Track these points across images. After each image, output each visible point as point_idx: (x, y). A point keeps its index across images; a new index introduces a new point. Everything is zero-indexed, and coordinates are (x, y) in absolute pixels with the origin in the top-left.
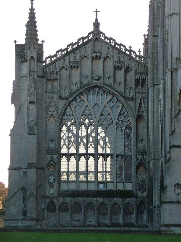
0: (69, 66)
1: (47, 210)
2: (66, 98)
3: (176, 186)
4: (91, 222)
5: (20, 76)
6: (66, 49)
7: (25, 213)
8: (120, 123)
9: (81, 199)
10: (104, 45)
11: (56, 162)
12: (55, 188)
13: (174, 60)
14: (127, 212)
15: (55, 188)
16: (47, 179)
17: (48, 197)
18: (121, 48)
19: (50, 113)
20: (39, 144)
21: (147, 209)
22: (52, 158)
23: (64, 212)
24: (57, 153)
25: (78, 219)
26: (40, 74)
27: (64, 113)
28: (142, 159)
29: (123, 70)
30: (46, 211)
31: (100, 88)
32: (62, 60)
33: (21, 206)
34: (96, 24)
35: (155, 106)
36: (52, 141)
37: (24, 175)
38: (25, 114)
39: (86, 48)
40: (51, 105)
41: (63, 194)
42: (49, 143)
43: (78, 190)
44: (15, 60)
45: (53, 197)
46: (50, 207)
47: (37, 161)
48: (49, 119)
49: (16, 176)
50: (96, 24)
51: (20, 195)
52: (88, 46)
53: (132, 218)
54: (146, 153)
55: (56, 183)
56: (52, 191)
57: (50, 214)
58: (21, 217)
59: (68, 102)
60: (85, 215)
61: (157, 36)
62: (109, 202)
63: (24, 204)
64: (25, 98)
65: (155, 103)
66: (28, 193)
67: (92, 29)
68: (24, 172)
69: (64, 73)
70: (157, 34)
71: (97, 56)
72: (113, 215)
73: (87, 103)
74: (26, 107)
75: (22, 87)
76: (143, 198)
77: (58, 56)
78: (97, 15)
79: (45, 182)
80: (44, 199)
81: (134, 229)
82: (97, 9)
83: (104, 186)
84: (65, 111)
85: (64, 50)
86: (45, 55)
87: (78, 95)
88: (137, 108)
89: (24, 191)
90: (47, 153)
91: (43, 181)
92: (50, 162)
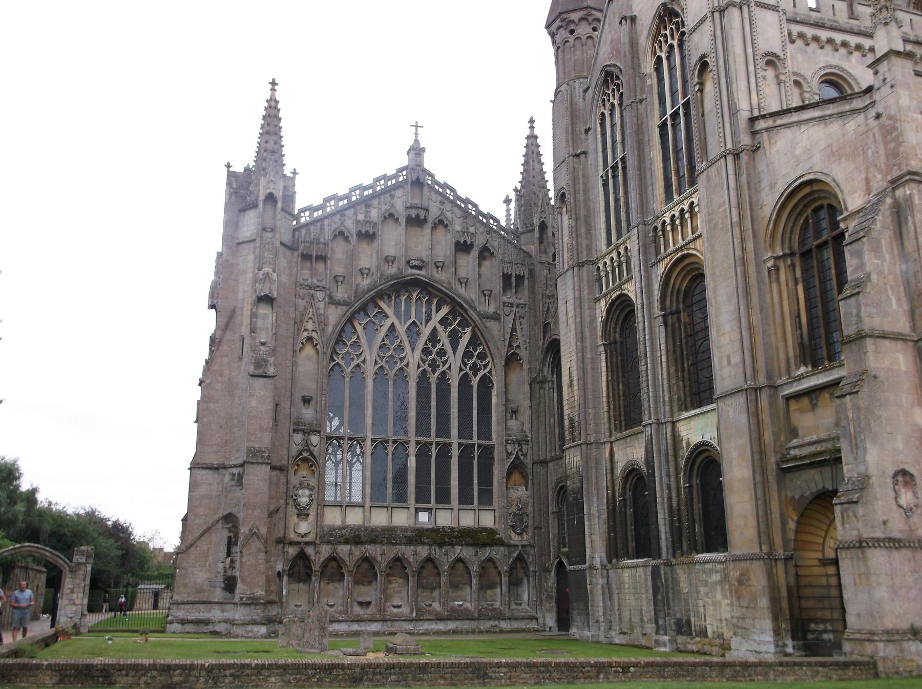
0: (354, 232)
1: (290, 576)
2: (346, 303)
3: (900, 478)
4: (399, 607)
5: (236, 241)
6: (347, 197)
7: (230, 584)
8: (468, 370)
9: (374, 550)
10: (434, 196)
11: (316, 453)
12: (312, 518)
13: (743, 124)
14: (486, 585)
15: (312, 518)
16: (292, 497)
17: (292, 543)
18: (467, 206)
19: (306, 334)
20: (277, 405)
21: (531, 574)
22: (307, 446)
23: (332, 581)
24: (319, 432)
25: (368, 599)
26: (287, 239)
27: (339, 340)
28: (520, 454)
29: (475, 252)
30: (285, 578)
32: (338, 216)
33: (221, 565)
34: (417, 151)
35: (587, 312)
36: (306, 401)
37: (233, 483)
38: (245, 330)
39: (392, 197)
40: (310, 316)
41: (331, 535)
42: (299, 406)
43: (367, 525)
44: (226, 204)
45: (307, 543)
46: (296, 569)
47: (273, 444)
48: (301, 349)
49: (210, 484)
50: (417, 151)
51: (221, 535)
52: (399, 193)
53: (497, 597)
54: (528, 441)
55: (314, 505)
56: (304, 527)
57: (295, 586)
58: (218, 594)
59: (351, 310)
60: (384, 591)
61: (585, 153)
62: (446, 557)
63: (229, 560)
64: (245, 292)
65: (586, 305)
66: (244, 530)
67: (404, 161)
68: (233, 475)
69: (339, 250)
70: (583, 150)
71: (418, 216)
72: (450, 591)
73: (392, 319)
74: (247, 313)
75: (241, 267)
76: (523, 546)
77: (329, 209)
78: (416, 134)
79: (287, 504)
80: (283, 548)
81: (503, 625)
82: (417, 122)
83: (429, 518)
84: (340, 336)
85: (342, 198)
86: (299, 204)
87: (373, 300)
88: (508, 337)
89: (230, 525)
90: (294, 431)
91: (282, 502)
92: (301, 454)
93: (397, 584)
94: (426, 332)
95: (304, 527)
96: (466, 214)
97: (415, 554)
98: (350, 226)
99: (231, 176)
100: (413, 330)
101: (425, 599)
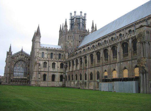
7: (6, 82)
9: (17, 80)
14: (25, 82)
27: (15, 64)
31: (22, 60)
34: (22, 49)
50: (22, 49)
51: (6, 79)
56: (12, 78)
58: (6, 82)
62: (22, 80)
64: (8, 61)
69: (15, 57)
86: (12, 54)
93: (19, 82)
94: (22, 64)
95: (12, 78)
96: (26, 54)
97: (20, 80)
98: (16, 56)
99: (7, 52)
100: (21, 64)
101: (21, 83)
